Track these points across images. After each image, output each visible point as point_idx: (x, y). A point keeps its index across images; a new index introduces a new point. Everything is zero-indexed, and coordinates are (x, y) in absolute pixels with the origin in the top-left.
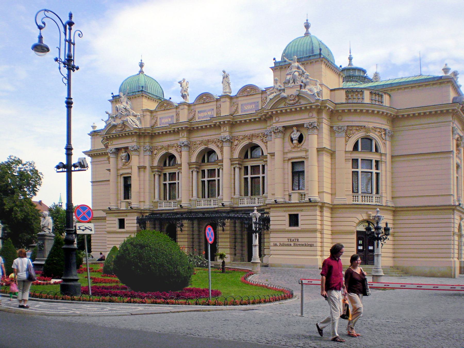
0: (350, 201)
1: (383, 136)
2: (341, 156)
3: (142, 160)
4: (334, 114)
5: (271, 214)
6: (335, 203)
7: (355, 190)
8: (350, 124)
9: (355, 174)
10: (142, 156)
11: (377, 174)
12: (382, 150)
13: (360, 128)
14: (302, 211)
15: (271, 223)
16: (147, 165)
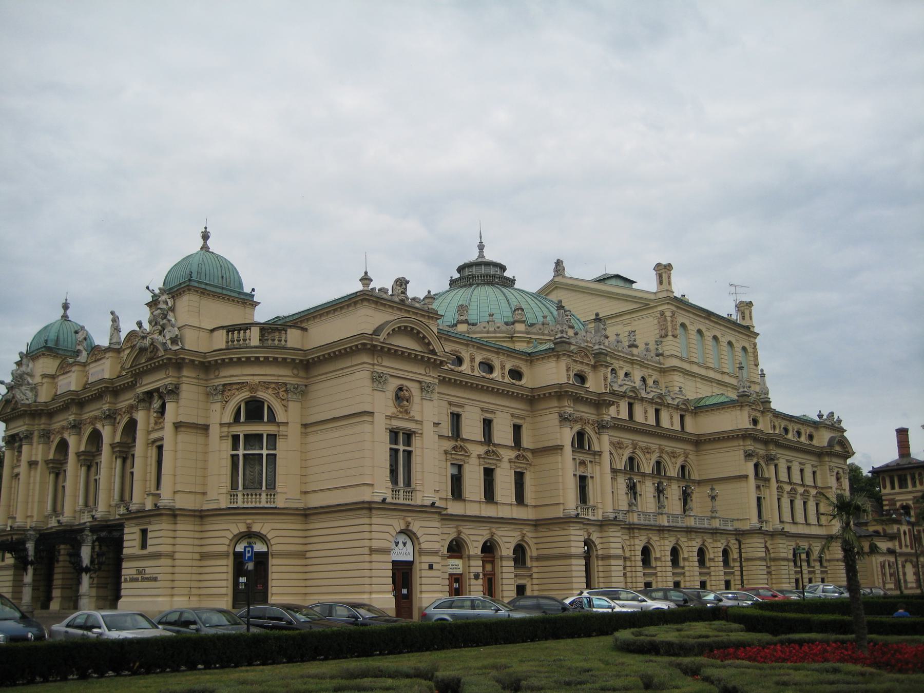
0: (224, 503)
1: (281, 394)
2: (215, 431)
3: (34, 452)
4: (207, 366)
5: (126, 531)
6: (205, 507)
7: (234, 485)
8: (228, 381)
9: (234, 458)
10: (35, 444)
11: (272, 458)
12: (281, 417)
13: (242, 385)
14: (150, 523)
15: (125, 544)
16: (39, 458)
